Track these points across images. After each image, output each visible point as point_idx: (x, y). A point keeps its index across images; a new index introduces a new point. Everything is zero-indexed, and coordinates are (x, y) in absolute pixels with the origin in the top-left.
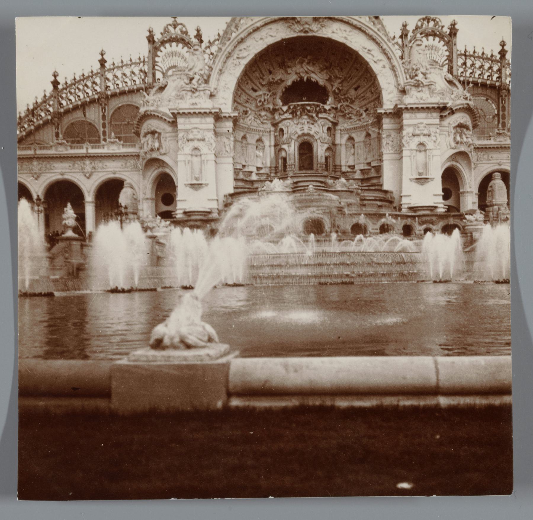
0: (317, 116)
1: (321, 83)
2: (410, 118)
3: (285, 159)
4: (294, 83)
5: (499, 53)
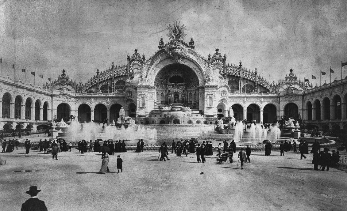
0: (180, 87)
1: (181, 77)
2: (207, 90)
3: (170, 99)
4: (173, 76)
5: (239, 66)
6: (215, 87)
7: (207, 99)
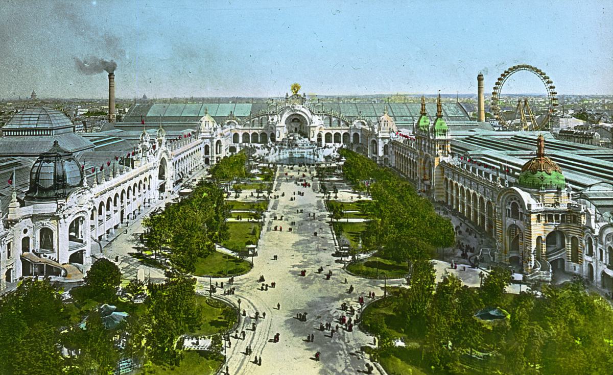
6: (315, 127)
7: (311, 132)
